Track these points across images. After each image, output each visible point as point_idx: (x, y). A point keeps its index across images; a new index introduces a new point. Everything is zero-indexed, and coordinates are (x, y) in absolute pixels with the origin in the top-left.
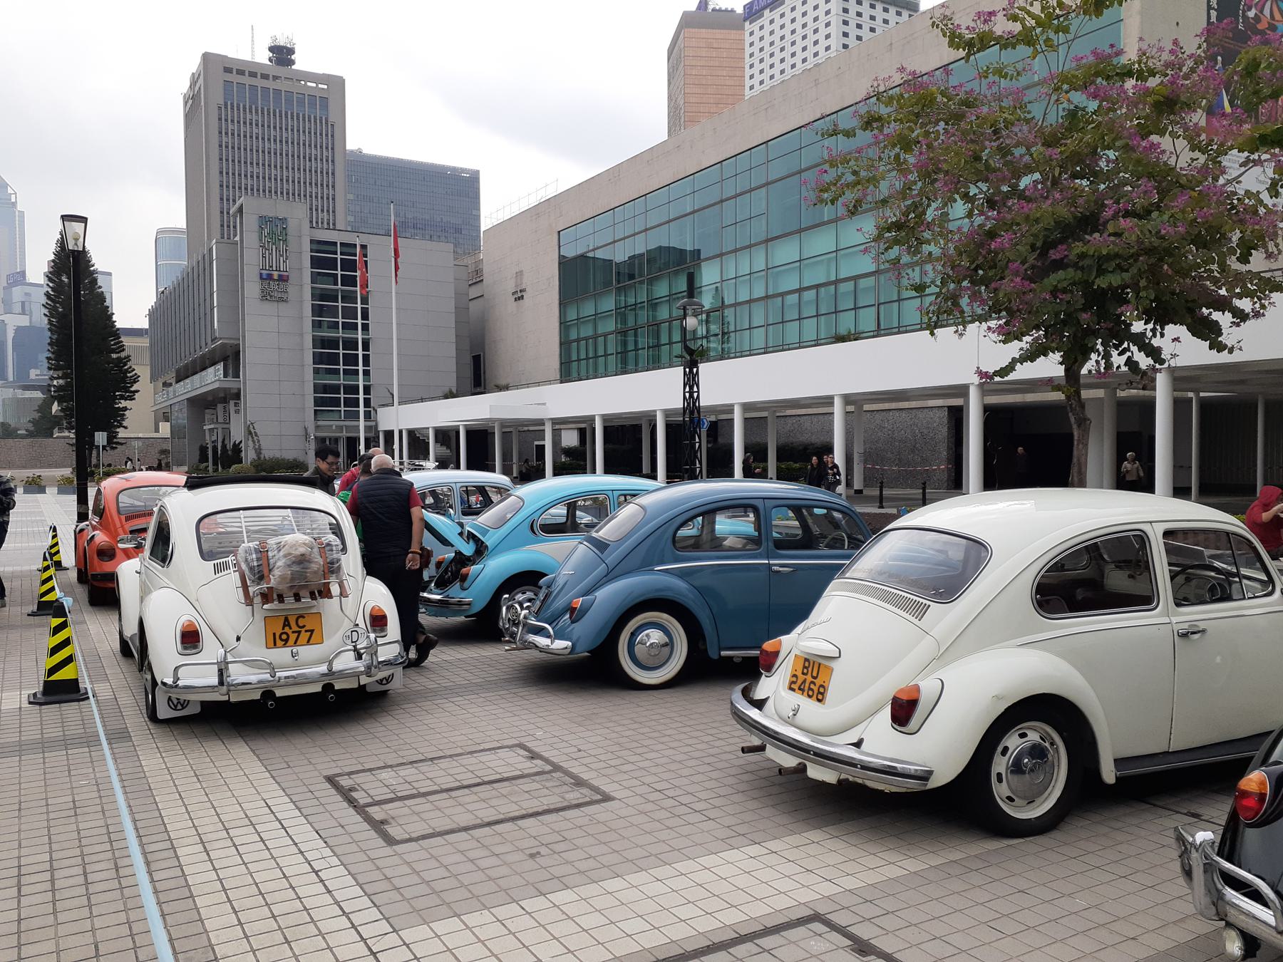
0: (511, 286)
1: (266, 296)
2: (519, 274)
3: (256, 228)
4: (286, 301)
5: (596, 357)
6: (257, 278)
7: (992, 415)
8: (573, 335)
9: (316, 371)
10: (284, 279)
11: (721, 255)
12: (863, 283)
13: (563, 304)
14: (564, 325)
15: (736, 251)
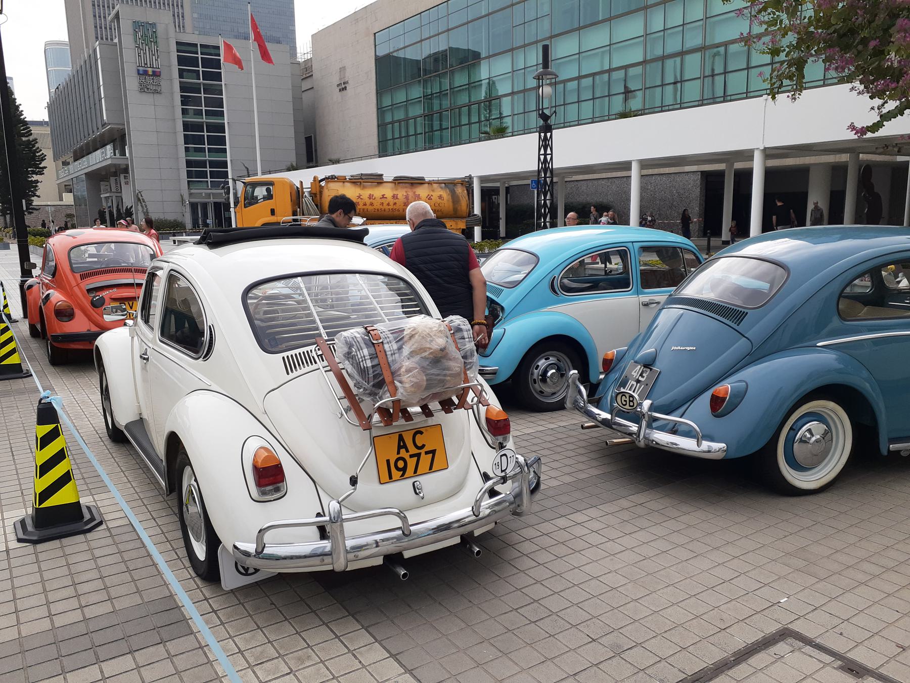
0: (336, 80)
1: (143, 89)
2: (342, 69)
3: (131, 31)
4: (159, 93)
5: (408, 136)
6: (135, 74)
7: (770, 175)
8: (388, 118)
9: (187, 149)
10: (156, 74)
11: (512, 50)
12: (632, 71)
13: (379, 93)
14: (381, 111)
15: (524, 46)
